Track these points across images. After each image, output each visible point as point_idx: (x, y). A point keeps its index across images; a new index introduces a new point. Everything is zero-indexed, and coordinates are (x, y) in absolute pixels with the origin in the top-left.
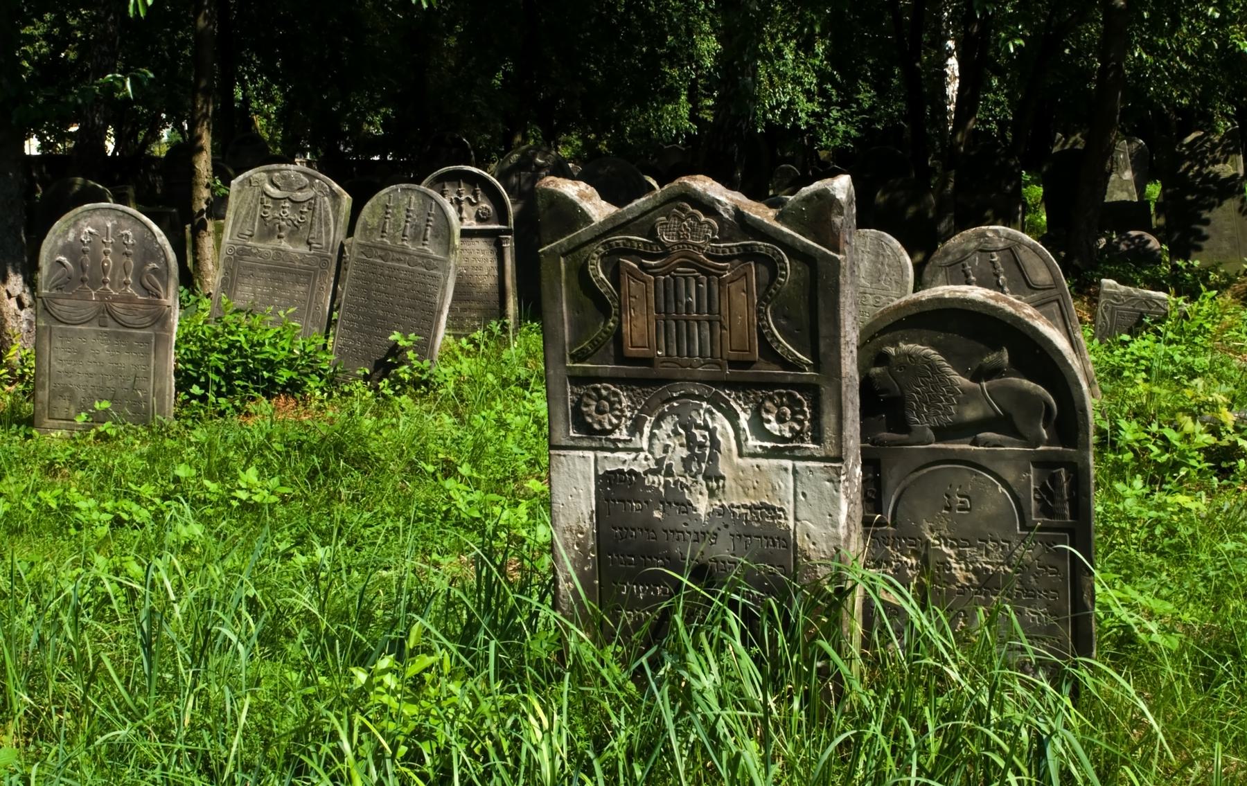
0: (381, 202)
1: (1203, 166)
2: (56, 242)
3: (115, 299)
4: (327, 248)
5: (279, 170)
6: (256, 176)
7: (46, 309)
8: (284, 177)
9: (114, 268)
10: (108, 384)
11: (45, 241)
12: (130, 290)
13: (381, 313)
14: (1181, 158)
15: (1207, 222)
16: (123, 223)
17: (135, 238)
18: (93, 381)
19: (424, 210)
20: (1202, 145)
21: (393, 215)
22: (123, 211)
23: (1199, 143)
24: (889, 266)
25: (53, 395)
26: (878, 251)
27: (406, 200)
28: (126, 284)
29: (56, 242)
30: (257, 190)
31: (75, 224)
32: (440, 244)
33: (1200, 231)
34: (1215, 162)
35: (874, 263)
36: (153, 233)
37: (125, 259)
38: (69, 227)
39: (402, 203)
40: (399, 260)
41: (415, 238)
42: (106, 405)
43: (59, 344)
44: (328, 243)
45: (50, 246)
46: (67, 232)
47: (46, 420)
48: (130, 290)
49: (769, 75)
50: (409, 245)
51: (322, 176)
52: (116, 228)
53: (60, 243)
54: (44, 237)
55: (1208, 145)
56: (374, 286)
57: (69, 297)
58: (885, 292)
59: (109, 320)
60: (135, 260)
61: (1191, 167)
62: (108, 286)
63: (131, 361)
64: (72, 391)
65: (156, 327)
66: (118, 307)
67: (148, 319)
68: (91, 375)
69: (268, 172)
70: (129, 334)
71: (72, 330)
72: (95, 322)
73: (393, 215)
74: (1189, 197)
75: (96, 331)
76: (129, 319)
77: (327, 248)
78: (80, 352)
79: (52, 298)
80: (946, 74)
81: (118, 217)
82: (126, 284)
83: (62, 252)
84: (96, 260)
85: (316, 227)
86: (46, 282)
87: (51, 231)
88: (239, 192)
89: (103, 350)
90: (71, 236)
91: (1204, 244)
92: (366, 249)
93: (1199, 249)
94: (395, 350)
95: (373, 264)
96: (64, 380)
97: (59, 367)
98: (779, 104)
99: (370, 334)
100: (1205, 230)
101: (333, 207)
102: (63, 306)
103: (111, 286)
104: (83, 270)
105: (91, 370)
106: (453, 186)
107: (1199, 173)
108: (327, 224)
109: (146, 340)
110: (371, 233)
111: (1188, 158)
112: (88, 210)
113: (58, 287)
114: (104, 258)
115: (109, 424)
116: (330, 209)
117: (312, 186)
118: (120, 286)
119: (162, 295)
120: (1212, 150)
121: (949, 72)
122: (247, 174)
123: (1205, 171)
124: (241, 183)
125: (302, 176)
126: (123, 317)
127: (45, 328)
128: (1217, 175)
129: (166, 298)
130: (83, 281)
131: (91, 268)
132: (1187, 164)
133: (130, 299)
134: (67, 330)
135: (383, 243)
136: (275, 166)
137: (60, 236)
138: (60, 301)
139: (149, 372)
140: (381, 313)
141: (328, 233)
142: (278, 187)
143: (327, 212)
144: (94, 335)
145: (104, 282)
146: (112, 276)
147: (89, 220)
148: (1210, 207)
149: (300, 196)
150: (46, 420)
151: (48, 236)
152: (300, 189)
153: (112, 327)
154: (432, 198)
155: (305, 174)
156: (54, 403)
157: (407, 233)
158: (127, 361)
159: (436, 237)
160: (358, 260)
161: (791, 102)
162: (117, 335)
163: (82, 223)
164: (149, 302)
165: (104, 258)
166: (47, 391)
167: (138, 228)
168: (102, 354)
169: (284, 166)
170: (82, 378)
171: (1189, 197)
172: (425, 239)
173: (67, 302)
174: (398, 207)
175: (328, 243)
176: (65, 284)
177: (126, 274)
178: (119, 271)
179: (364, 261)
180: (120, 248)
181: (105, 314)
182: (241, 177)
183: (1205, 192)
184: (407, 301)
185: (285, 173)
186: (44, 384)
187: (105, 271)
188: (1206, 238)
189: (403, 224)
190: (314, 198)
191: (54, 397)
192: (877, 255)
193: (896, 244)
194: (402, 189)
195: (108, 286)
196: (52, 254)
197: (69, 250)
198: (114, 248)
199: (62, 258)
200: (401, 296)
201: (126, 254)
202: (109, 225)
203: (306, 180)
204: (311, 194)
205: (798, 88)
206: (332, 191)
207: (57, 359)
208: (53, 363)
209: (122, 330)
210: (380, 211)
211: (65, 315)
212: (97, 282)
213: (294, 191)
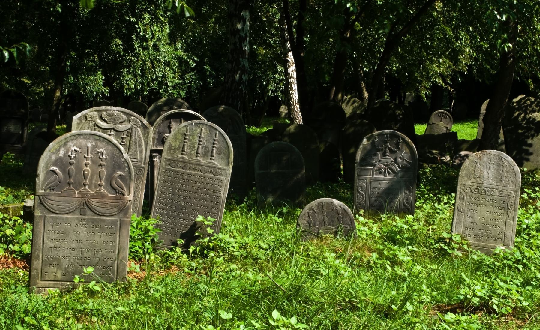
0: (181, 132)
1: (526, 114)
2: (50, 157)
3: (93, 196)
4: (141, 161)
5: (106, 110)
6: (91, 114)
7: (42, 203)
8: (109, 115)
9: (92, 175)
10: (86, 255)
11: (43, 157)
12: (103, 190)
13: (182, 203)
14: (514, 110)
15: (531, 145)
16: (99, 144)
17: (107, 154)
18: (75, 253)
19: (211, 136)
20: (525, 103)
21: (189, 140)
22: (100, 136)
23: (523, 101)
24: (507, 172)
25: (45, 264)
26: (500, 164)
27: (199, 130)
28: (100, 186)
29: (50, 157)
30: (92, 123)
31: (65, 144)
32: (222, 159)
33: (527, 150)
34: (534, 111)
35: (497, 170)
36: (121, 151)
37: (100, 169)
38: (60, 147)
39: (195, 133)
40: (194, 169)
41: (205, 155)
42: (90, 270)
43: (50, 228)
44: (141, 158)
45: (46, 160)
46: (59, 150)
47: (39, 281)
48: (103, 190)
49: (151, 60)
50: (201, 160)
51: (135, 114)
52: (94, 147)
53: (54, 157)
54: (42, 153)
55: (528, 102)
56: (177, 186)
57: (59, 195)
58: (506, 188)
59: (88, 212)
60: (107, 169)
61: (519, 115)
62: (87, 187)
63: (103, 239)
64: (59, 261)
65: (121, 215)
66: (94, 202)
67: (116, 210)
68: (73, 249)
69: (98, 111)
70: (102, 220)
71: (61, 218)
72: (78, 212)
73: (189, 140)
74: (520, 131)
75: (78, 219)
76: (101, 210)
77: (141, 161)
78: (66, 233)
79: (46, 196)
80: (288, 61)
81: (96, 140)
82: (100, 186)
83: (55, 164)
84: (79, 168)
85: (133, 147)
86: (43, 185)
87: (47, 149)
88: (79, 124)
89: (83, 232)
90: (62, 153)
91: (531, 157)
92: (172, 162)
93: (528, 160)
94: (195, 227)
95: (176, 172)
96: (54, 253)
97: (50, 244)
98: (157, 77)
99: (175, 217)
100: (531, 150)
101: (144, 135)
102: (55, 201)
103: (89, 187)
104: (70, 176)
105: (73, 245)
106: (177, 122)
107: (524, 118)
108: (140, 146)
109: (113, 224)
110: (175, 152)
111: (518, 109)
112: (75, 135)
113: (51, 189)
114: (85, 168)
115: (93, 283)
116: (142, 136)
117: (129, 121)
118: (96, 187)
119: (126, 194)
120: (530, 106)
121: (290, 60)
122: (84, 112)
123: (528, 116)
124: (80, 119)
125: (122, 115)
126: (98, 209)
127: (40, 217)
128: (534, 119)
129: (129, 195)
130: (69, 184)
131: (75, 175)
132: (518, 113)
133: (103, 196)
134: (57, 218)
135: (183, 158)
136: (103, 107)
137: (54, 153)
138: (52, 198)
139: (115, 246)
140: (182, 203)
141: (141, 152)
142: (106, 122)
143: (140, 138)
144: (76, 221)
145: (85, 185)
146: (91, 180)
147: (75, 142)
148: (533, 136)
149: (121, 127)
150: (39, 281)
151: (45, 153)
152: (121, 123)
153: (89, 215)
154: (216, 129)
155: (124, 113)
156: (46, 269)
157: (200, 152)
158: (99, 238)
159: (220, 154)
160: (166, 169)
161: (164, 76)
162: (93, 221)
163: (70, 144)
164: (116, 198)
165: (85, 168)
166: (41, 261)
167: (110, 148)
168: (82, 234)
169: (109, 107)
170: (67, 252)
171: (520, 131)
172: (212, 156)
173: (57, 198)
174: (193, 135)
175: (141, 158)
176: (55, 187)
177: (101, 179)
178: (96, 177)
179: (170, 170)
180: (97, 161)
181: (85, 206)
182: (79, 115)
183: (528, 129)
184: (201, 196)
185: (110, 112)
186: (38, 256)
187: (85, 177)
188: (531, 154)
189: (196, 146)
190: (131, 129)
191: (46, 265)
192: (499, 165)
193: (510, 159)
194: (196, 124)
195: (87, 187)
196: (47, 165)
197: (59, 162)
198: (92, 161)
199: (55, 168)
200: (197, 192)
201: (101, 165)
202: (89, 145)
203: (125, 117)
204: (129, 126)
205: (168, 68)
206: (143, 124)
207: (49, 238)
208: (46, 241)
209: (96, 217)
210: (181, 138)
211: (56, 207)
212: (79, 185)
213: (117, 124)
